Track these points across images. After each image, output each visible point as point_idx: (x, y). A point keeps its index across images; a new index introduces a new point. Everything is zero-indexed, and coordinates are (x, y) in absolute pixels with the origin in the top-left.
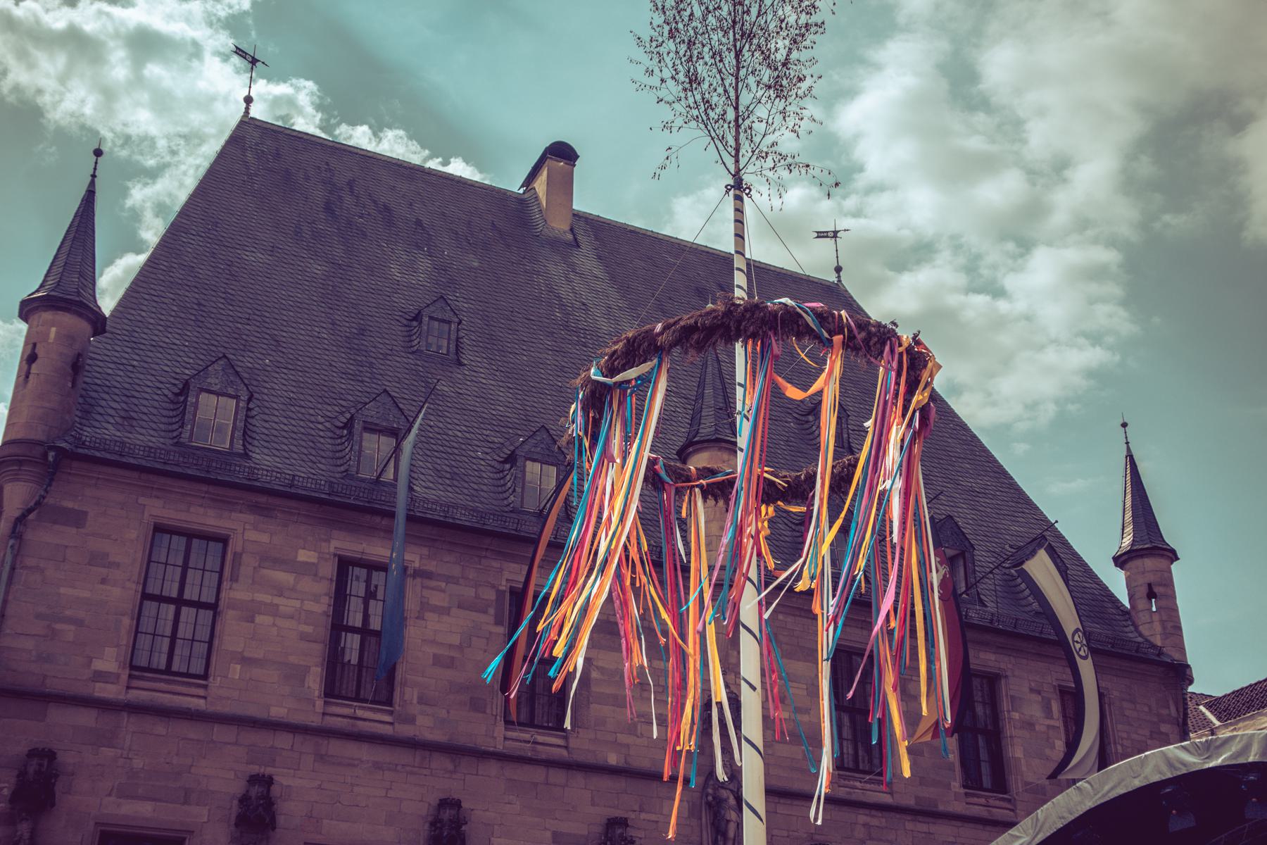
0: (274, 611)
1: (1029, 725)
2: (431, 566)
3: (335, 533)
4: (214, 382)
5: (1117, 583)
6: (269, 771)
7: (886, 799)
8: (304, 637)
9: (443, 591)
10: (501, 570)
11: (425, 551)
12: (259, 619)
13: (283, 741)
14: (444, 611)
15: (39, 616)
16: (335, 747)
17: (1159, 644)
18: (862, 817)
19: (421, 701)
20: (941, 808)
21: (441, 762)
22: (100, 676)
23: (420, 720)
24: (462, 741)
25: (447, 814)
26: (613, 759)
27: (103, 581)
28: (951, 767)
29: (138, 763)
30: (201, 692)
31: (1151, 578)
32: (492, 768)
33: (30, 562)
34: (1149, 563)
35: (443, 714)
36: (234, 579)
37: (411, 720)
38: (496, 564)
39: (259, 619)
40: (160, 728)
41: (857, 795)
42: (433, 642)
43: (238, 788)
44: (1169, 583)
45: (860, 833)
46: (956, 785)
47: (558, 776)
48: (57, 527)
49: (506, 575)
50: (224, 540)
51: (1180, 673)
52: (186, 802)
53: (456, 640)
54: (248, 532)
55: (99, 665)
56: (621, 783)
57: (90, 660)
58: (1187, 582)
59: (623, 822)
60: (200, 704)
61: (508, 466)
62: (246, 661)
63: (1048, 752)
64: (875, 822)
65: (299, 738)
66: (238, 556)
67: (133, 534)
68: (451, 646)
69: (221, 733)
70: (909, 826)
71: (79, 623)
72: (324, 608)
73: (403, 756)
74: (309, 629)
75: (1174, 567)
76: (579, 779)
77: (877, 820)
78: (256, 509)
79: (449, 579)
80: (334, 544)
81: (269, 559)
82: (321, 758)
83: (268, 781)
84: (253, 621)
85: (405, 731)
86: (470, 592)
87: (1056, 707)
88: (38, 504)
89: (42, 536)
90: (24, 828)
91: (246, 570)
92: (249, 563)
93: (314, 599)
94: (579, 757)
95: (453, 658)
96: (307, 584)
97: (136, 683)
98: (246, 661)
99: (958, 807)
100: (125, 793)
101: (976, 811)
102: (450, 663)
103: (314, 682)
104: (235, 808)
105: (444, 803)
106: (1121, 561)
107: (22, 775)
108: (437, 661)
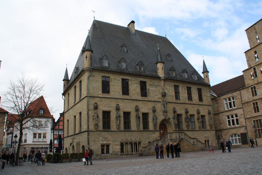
1: (195, 93)
2: (132, 79)
3: (121, 76)
4: (105, 58)
5: (202, 75)
6: (118, 104)
7: (181, 102)
8: (119, 88)
9: (133, 82)
10: (139, 79)
11: (131, 77)
12: (114, 86)
13: (119, 100)
14: (133, 84)
15: (92, 88)
16: (124, 100)
17: (207, 82)
18: (178, 104)
19: (132, 95)
20: (186, 103)
21: (135, 101)
22: (99, 94)
23: (133, 97)
24: (137, 99)
25: (137, 107)
26: (153, 100)
27: (98, 83)
28: (187, 98)
29: (105, 104)
30: (109, 95)
31: (206, 75)
32: (140, 102)
33: (90, 82)
34: (206, 73)
35: (135, 96)
36: (111, 82)
37: (132, 97)
38: (138, 78)
39: (114, 86)
40: (106, 99)
41: (178, 102)
42: (133, 88)
43: (115, 106)
44: (208, 75)
45: (178, 106)
46: (187, 100)
47: (147, 102)
48: (92, 77)
49: (139, 79)
50: (109, 77)
51: (210, 85)
52: (110, 107)
53: (135, 87)
54: (112, 76)
55: (99, 93)
56: (154, 102)
57: (98, 93)
58: (210, 75)
59: (155, 107)
60: (109, 97)
61: (137, 66)
62: (114, 91)
63: (196, 96)
64: (179, 105)
65: (121, 100)
66: (111, 79)
67: (100, 78)
68: (134, 88)
69: (113, 100)
70: (183, 105)
71: (96, 88)
72: (121, 85)
73: (131, 101)
74: (119, 87)
75: (209, 73)
76: (149, 102)
77: (180, 105)
78: (112, 74)
79: (134, 80)
80: (121, 77)
81: (114, 79)
82: (123, 102)
83: (118, 105)
84: (114, 87)
85: (131, 98)
86: (136, 82)
87: (197, 91)
88: (91, 75)
89: (91, 78)
90: (96, 111)
91: (112, 81)
92: (112, 80)
93: (120, 84)
94: (149, 100)
95: (135, 90)
96: (119, 82)
97: (103, 95)
98: (114, 91)
99: (188, 103)
100: (104, 107)
101: (189, 103)
102: (135, 90)
103: (121, 93)
104: (115, 108)
105: (136, 106)
106: (203, 73)
107: (94, 106)
108: (133, 90)
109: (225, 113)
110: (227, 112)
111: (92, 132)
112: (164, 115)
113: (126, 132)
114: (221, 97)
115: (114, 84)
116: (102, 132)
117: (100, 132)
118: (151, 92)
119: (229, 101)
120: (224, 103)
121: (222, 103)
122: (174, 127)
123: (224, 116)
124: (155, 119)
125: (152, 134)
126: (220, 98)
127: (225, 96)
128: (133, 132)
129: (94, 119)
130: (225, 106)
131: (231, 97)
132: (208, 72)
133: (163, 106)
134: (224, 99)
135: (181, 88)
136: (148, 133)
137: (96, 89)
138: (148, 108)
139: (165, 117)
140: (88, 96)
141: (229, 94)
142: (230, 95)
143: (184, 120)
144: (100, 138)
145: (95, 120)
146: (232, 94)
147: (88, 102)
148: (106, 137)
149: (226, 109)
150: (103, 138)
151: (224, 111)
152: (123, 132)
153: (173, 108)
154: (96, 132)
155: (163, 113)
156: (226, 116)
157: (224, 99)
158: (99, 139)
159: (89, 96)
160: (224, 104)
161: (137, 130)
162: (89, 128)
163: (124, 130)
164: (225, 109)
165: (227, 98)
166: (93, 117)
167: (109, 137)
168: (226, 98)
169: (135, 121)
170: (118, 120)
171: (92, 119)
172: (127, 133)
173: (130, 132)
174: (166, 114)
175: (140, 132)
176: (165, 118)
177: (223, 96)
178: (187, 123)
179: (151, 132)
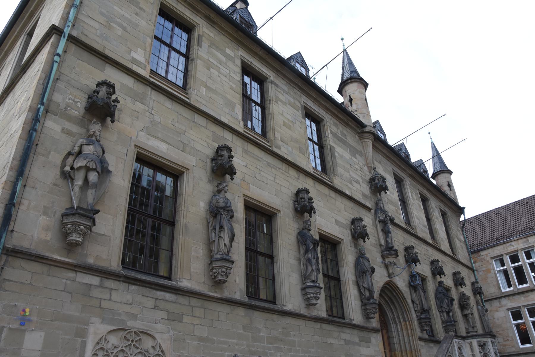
0: (218, 70)
109: (504, 301)
110: (511, 298)
111: (36, 267)
112: (386, 266)
113: (257, 314)
114: (483, 253)
115: (211, 60)
116: (110, 283)
117: (95, 280)
118: (339, 161)
119: (513, 262)
120: (494, 269)
121: (488, 271)
122: (416, 323)
123: (501, 309)
124: (363, 271)
125: (359, 345)
126: (480, 256)
127: (498, 251)
128: (289, 321)
129: (67, 176)
130: (501, 279)
131: (522, 250)
132: (450, 173)
133: (379, 227)
134: (492, 258)
135: (408, 187)
136: (348, 335)
137: (119, 31)
138: (339, 219)
139: (390, 276)
140: (67, 31)
141: (513, 243)
142: (518, 245)
143: (434, 300)
144: (91, 329)
145: (79, 182)
146: (525, 239)
147: (57, 58)
148: (137, 325)
149: (506, 289)
150: (110, 332)
151: (497, 295)
152: (241, 311)
153: (403, 247)
154: (71, 274)
155: (383, 257)
156: (508, 310)
157: (492, 258)
158: (82, 334)
159: (72, 39)
160: (495, 274)
161: (303, 311)
162: (19, 262)
163: (246, 299)
164: (500, 288)
165: (507, 254)
166: (70, 159)
167: (158, 326)
168: (502, 255)
169: (294, 262)
170: (222, 227)
171: (54, 174)
172: (259, 320)
173: (275, 317)
174: (395, 260)
175: (318, 325)
176: (388, 279)
177: (490, 251)
178: (445, 314)
179: (356, 332)
